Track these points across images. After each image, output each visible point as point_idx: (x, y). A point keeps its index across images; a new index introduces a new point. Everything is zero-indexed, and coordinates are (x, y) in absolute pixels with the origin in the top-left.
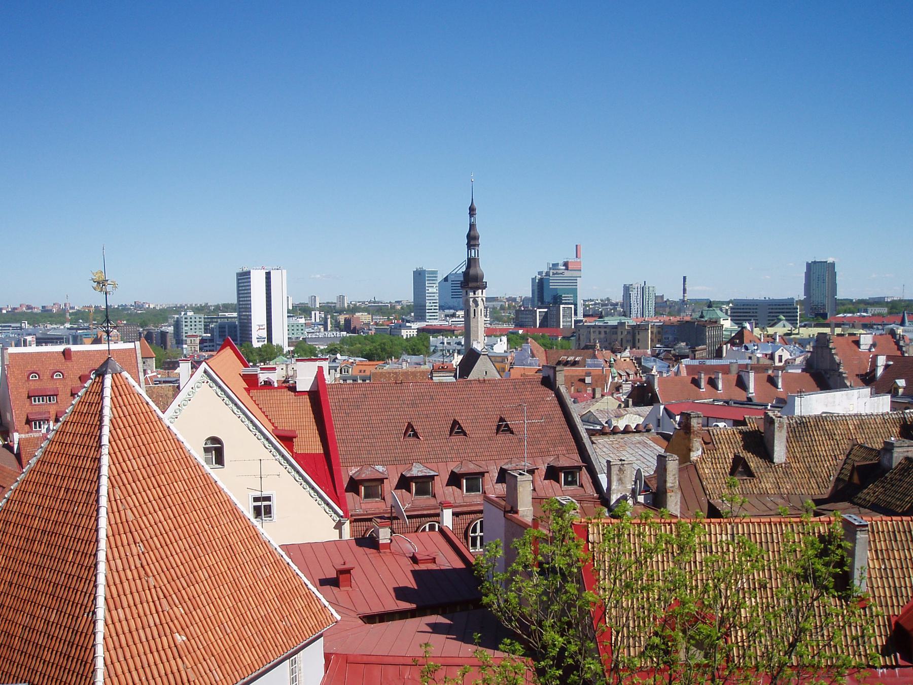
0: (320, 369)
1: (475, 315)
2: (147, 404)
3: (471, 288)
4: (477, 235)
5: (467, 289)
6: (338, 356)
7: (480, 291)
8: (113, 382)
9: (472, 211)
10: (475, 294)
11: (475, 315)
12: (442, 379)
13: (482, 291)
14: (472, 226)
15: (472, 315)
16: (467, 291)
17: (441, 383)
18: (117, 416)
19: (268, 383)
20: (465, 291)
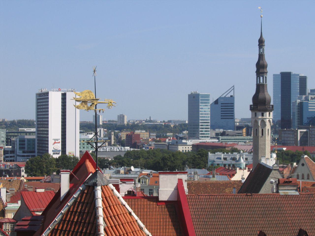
0: (180, 181)
1: (262, 135)
2: (130, 214)
3: (260, 111)
4: (265, 64)
5: (256, 111)
6: (132, 168)
7: (268, 113)
8: (103, 194)
9: (261, 43)
10: (263, 115)
11: (262, 135)
12: (287, 192)
13: (269, 114)
14: (261, 56)
15: (260, 134)
16: (256, 114)
17: (286, 196)
18: (109, 225)
19: (132, 193)
20: (254, 113)
